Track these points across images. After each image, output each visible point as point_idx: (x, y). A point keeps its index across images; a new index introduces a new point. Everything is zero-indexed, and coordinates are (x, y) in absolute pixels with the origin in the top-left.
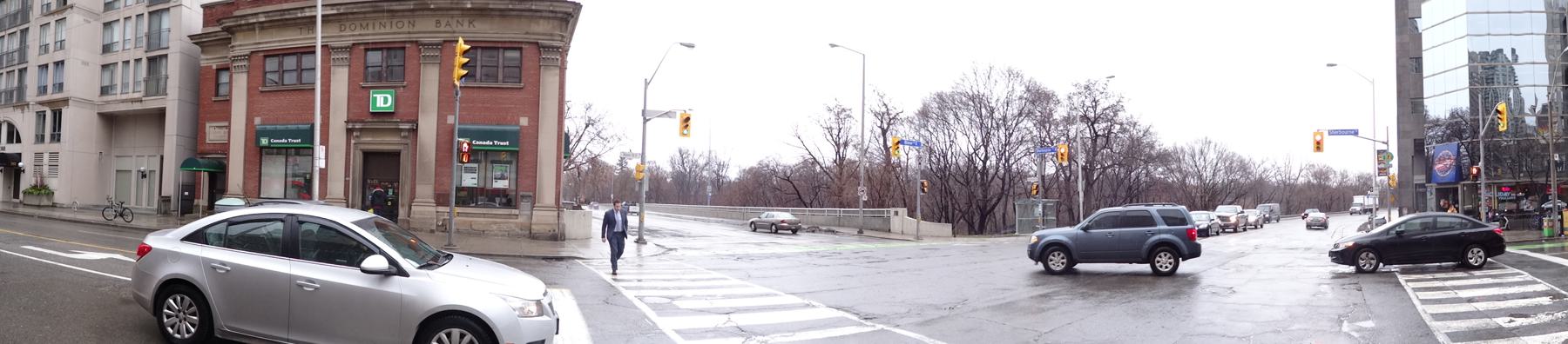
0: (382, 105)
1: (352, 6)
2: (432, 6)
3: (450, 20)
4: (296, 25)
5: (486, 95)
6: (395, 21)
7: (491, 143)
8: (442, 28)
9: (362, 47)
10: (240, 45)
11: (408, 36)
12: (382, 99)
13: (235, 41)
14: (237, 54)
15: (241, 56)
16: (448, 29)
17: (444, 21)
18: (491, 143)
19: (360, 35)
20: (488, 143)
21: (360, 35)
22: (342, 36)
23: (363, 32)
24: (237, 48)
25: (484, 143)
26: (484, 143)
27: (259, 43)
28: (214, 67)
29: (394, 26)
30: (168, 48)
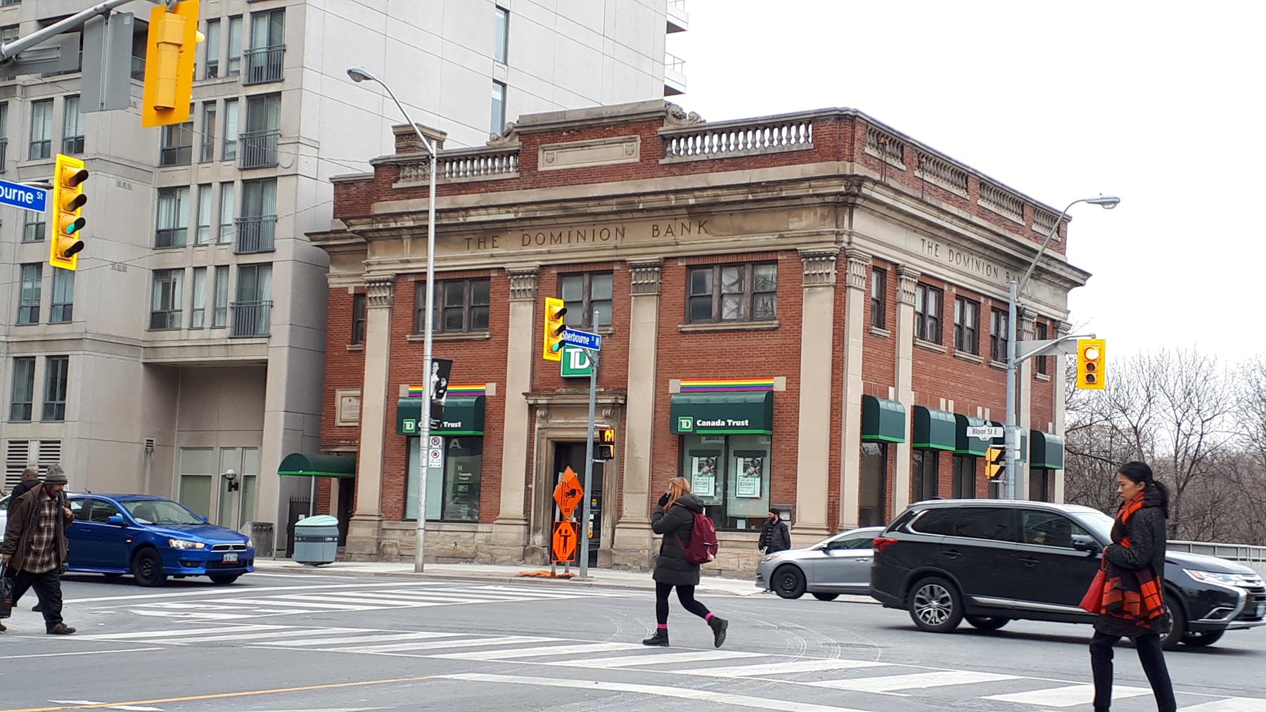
1: (534, 207)
2: (641, 206)
3: (672, 222)
4: (460, 233)
5: (725, 344)
6: (598, 229)
7: (723, 424)
8: (660, 239)
9: (554, 271)
10: (379, 263)
11: (614, 252)
13: (373, 254)
15: (380, 281)
16: (670, 238)
17: (663, 227)
18: (723, 424)
19: (549, 252)
21: (549, 252)
22: (524, 254)
23: (554, 247)
24: (374, 268)
25: (714, 424)
26: (714, 424)
27: (408, 261)
28: (351, 291)
29: (597, 237)
30: (273, 251)
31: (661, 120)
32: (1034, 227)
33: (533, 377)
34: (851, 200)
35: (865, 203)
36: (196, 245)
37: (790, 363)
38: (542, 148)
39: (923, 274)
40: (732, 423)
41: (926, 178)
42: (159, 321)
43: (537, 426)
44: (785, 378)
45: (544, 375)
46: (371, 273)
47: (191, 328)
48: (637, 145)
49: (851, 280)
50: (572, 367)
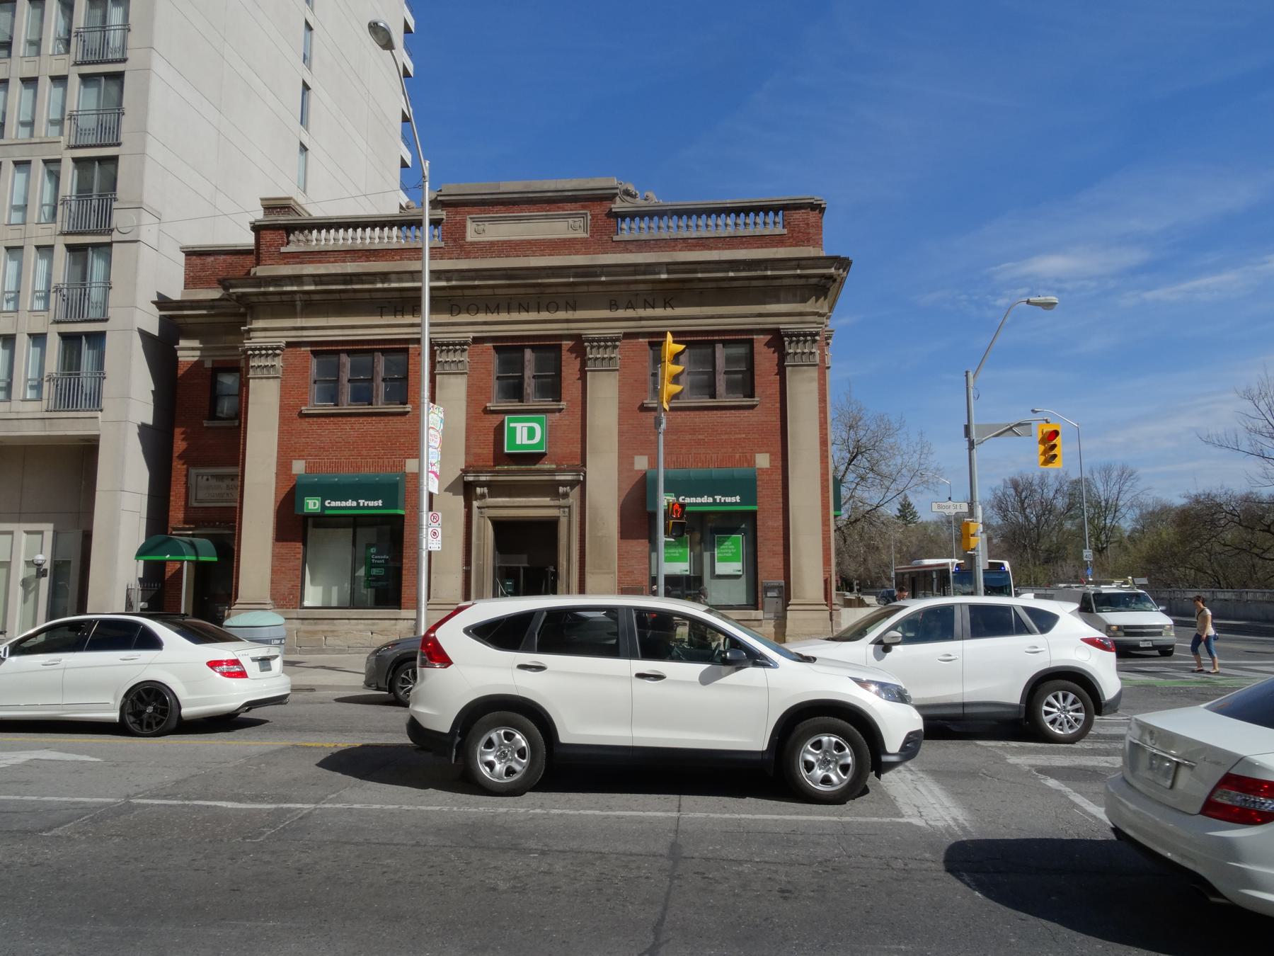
0: (526, 442)
12: (525, 430)
14: (258, 345)
18: (711, 500)
20: (705, 499)
30: (106, 320)
31: (611, 198)
33: (467, 453)
38: (471, 218)
40: (720, 499)
43: (475, 504)
44: (768, 455)
45: (479, 451)
46: (253, 340)
50: (518, 442)
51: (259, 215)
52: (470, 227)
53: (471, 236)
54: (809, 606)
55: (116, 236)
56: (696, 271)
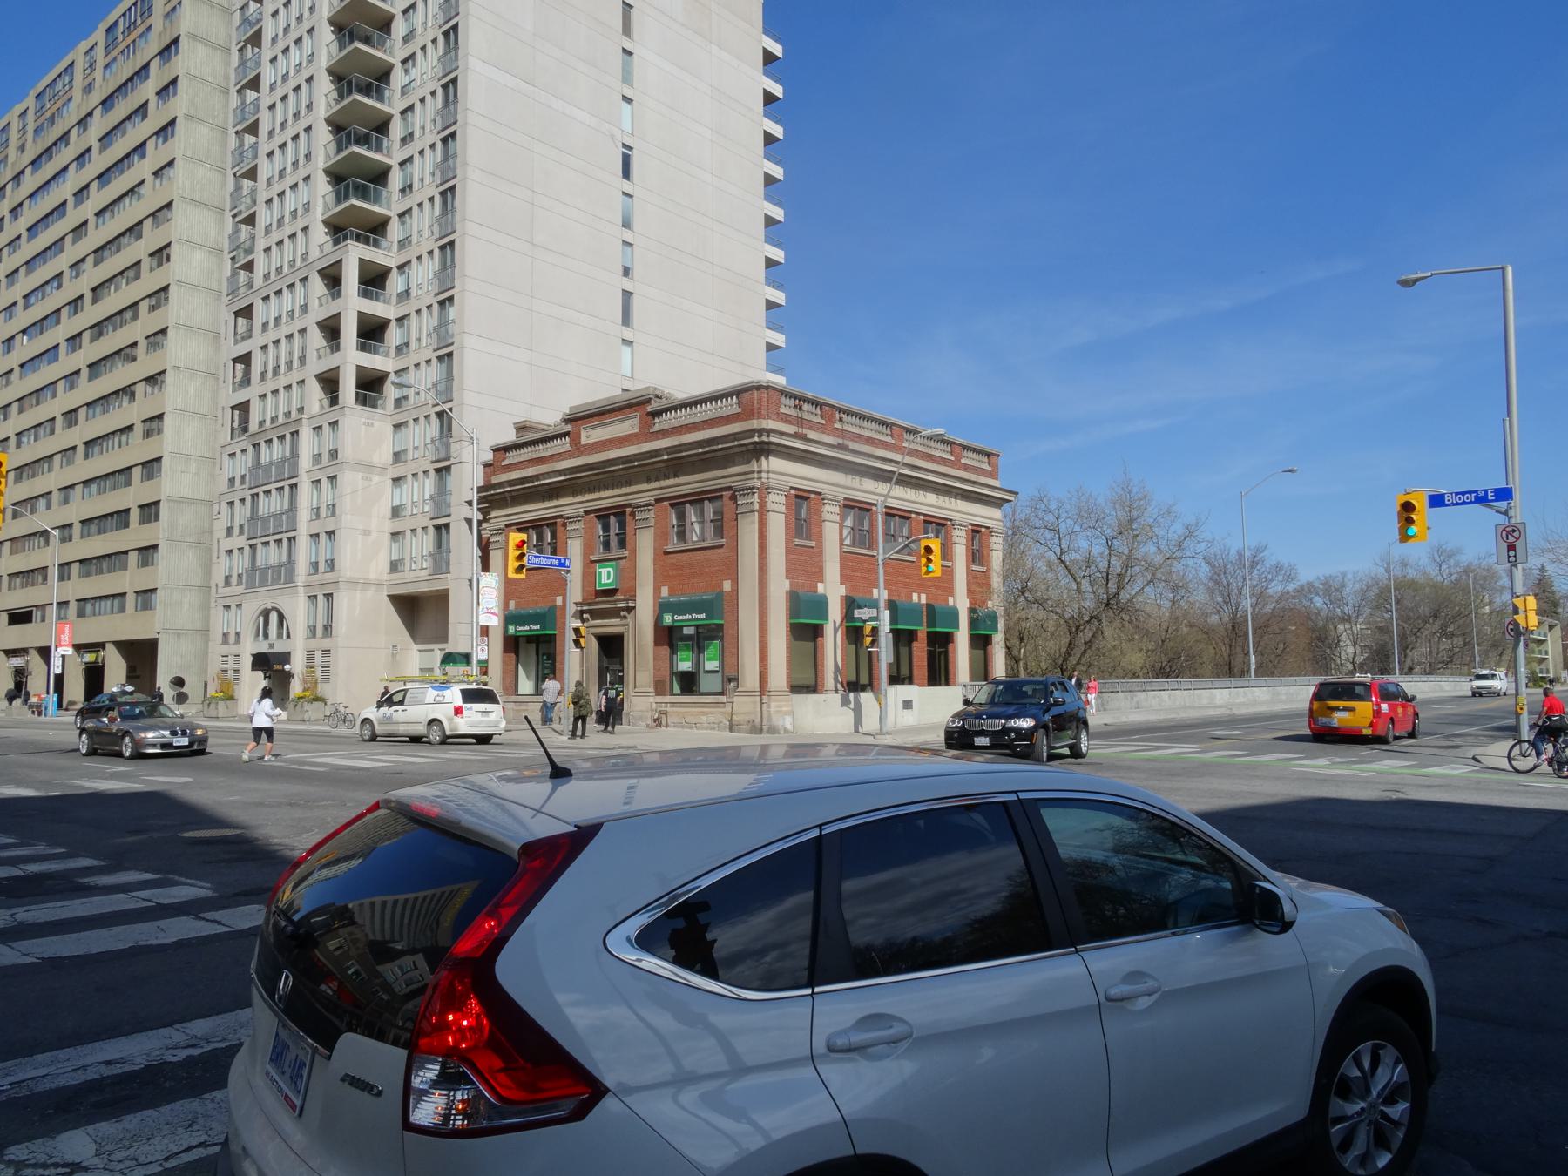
10: (495, 518)
31: (648, 401)
32: (963, 461)
34: (766, 447)
35: (778, 449)
36: (412, 515)
37: (732, 569)
39: (845, 499)
41: (845, 428)
42: (395, 566)
47: (411, 570)
48: (636, 421)
49: (769, 506)
51: (510, 436)
52: (583, 434)
53: (584, 441)
54: (749, 693)
55: (452, 461)
56: (681, 452)
